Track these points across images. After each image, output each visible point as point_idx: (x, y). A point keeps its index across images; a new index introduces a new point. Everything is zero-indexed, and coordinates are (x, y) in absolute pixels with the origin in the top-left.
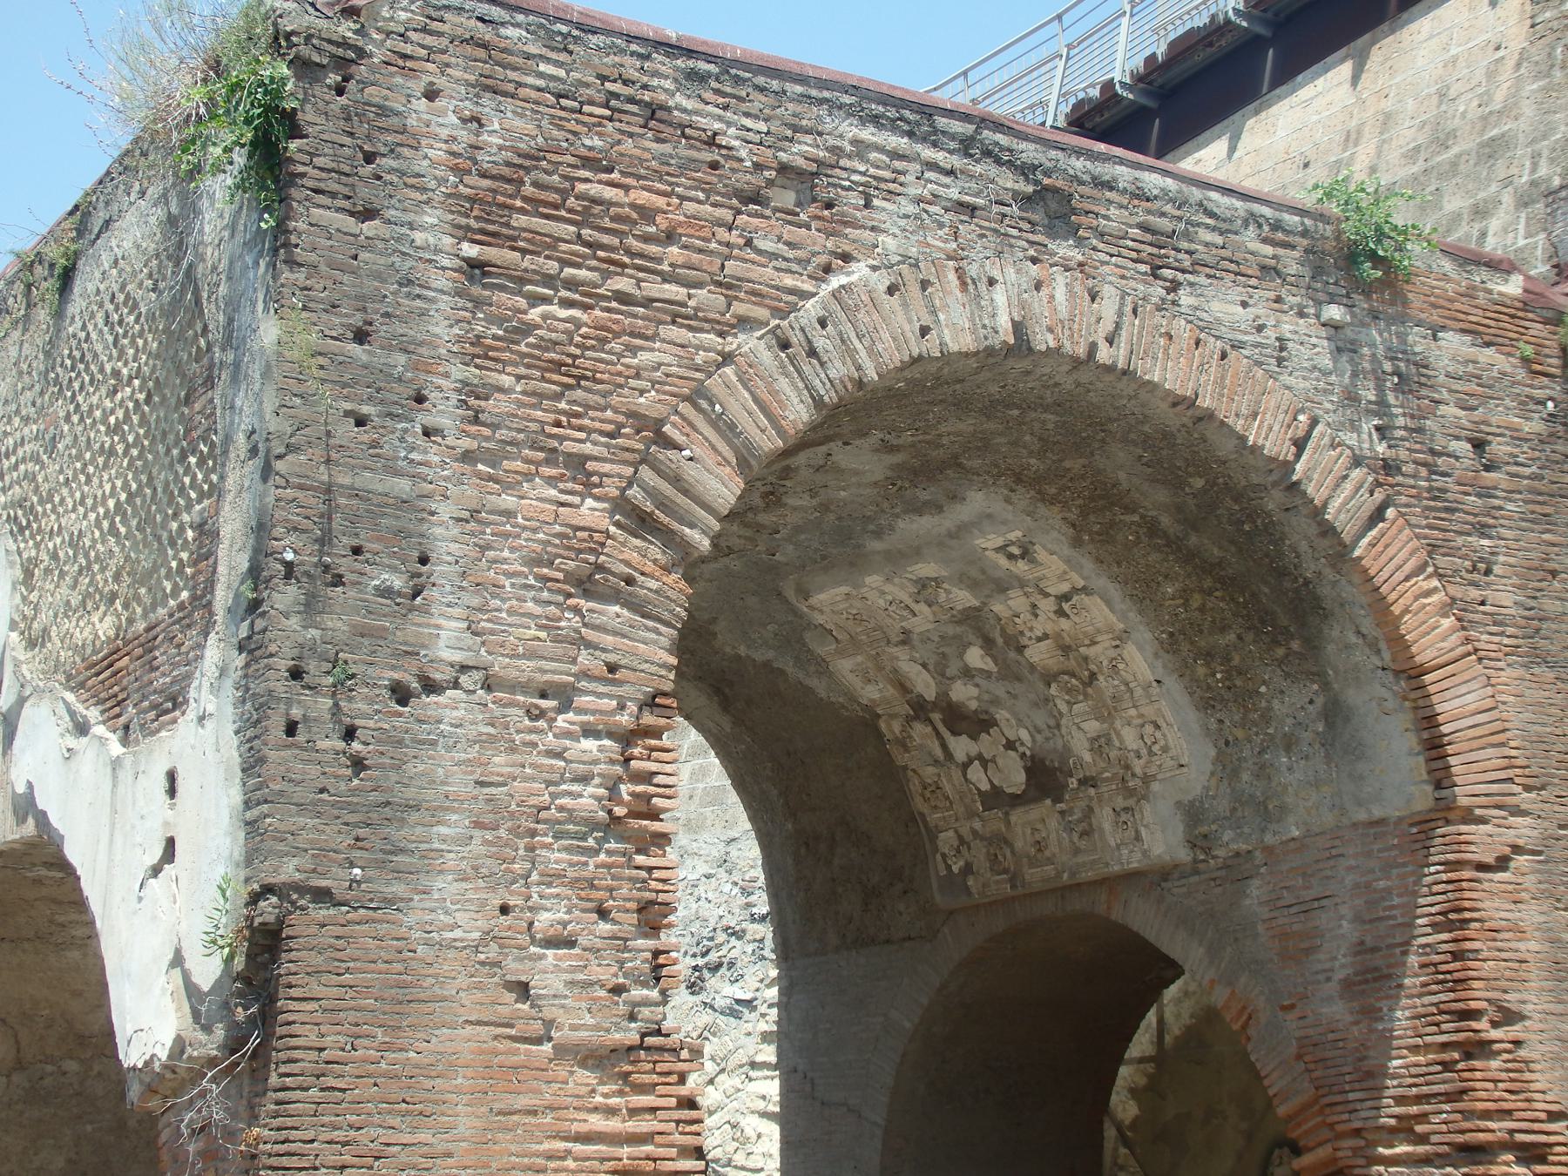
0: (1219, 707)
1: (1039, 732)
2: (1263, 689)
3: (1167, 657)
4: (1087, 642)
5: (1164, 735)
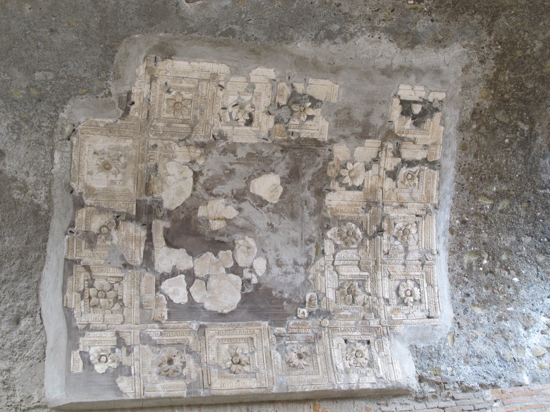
1: (279, 264)
2: (516, 279)
4: (395, 204)
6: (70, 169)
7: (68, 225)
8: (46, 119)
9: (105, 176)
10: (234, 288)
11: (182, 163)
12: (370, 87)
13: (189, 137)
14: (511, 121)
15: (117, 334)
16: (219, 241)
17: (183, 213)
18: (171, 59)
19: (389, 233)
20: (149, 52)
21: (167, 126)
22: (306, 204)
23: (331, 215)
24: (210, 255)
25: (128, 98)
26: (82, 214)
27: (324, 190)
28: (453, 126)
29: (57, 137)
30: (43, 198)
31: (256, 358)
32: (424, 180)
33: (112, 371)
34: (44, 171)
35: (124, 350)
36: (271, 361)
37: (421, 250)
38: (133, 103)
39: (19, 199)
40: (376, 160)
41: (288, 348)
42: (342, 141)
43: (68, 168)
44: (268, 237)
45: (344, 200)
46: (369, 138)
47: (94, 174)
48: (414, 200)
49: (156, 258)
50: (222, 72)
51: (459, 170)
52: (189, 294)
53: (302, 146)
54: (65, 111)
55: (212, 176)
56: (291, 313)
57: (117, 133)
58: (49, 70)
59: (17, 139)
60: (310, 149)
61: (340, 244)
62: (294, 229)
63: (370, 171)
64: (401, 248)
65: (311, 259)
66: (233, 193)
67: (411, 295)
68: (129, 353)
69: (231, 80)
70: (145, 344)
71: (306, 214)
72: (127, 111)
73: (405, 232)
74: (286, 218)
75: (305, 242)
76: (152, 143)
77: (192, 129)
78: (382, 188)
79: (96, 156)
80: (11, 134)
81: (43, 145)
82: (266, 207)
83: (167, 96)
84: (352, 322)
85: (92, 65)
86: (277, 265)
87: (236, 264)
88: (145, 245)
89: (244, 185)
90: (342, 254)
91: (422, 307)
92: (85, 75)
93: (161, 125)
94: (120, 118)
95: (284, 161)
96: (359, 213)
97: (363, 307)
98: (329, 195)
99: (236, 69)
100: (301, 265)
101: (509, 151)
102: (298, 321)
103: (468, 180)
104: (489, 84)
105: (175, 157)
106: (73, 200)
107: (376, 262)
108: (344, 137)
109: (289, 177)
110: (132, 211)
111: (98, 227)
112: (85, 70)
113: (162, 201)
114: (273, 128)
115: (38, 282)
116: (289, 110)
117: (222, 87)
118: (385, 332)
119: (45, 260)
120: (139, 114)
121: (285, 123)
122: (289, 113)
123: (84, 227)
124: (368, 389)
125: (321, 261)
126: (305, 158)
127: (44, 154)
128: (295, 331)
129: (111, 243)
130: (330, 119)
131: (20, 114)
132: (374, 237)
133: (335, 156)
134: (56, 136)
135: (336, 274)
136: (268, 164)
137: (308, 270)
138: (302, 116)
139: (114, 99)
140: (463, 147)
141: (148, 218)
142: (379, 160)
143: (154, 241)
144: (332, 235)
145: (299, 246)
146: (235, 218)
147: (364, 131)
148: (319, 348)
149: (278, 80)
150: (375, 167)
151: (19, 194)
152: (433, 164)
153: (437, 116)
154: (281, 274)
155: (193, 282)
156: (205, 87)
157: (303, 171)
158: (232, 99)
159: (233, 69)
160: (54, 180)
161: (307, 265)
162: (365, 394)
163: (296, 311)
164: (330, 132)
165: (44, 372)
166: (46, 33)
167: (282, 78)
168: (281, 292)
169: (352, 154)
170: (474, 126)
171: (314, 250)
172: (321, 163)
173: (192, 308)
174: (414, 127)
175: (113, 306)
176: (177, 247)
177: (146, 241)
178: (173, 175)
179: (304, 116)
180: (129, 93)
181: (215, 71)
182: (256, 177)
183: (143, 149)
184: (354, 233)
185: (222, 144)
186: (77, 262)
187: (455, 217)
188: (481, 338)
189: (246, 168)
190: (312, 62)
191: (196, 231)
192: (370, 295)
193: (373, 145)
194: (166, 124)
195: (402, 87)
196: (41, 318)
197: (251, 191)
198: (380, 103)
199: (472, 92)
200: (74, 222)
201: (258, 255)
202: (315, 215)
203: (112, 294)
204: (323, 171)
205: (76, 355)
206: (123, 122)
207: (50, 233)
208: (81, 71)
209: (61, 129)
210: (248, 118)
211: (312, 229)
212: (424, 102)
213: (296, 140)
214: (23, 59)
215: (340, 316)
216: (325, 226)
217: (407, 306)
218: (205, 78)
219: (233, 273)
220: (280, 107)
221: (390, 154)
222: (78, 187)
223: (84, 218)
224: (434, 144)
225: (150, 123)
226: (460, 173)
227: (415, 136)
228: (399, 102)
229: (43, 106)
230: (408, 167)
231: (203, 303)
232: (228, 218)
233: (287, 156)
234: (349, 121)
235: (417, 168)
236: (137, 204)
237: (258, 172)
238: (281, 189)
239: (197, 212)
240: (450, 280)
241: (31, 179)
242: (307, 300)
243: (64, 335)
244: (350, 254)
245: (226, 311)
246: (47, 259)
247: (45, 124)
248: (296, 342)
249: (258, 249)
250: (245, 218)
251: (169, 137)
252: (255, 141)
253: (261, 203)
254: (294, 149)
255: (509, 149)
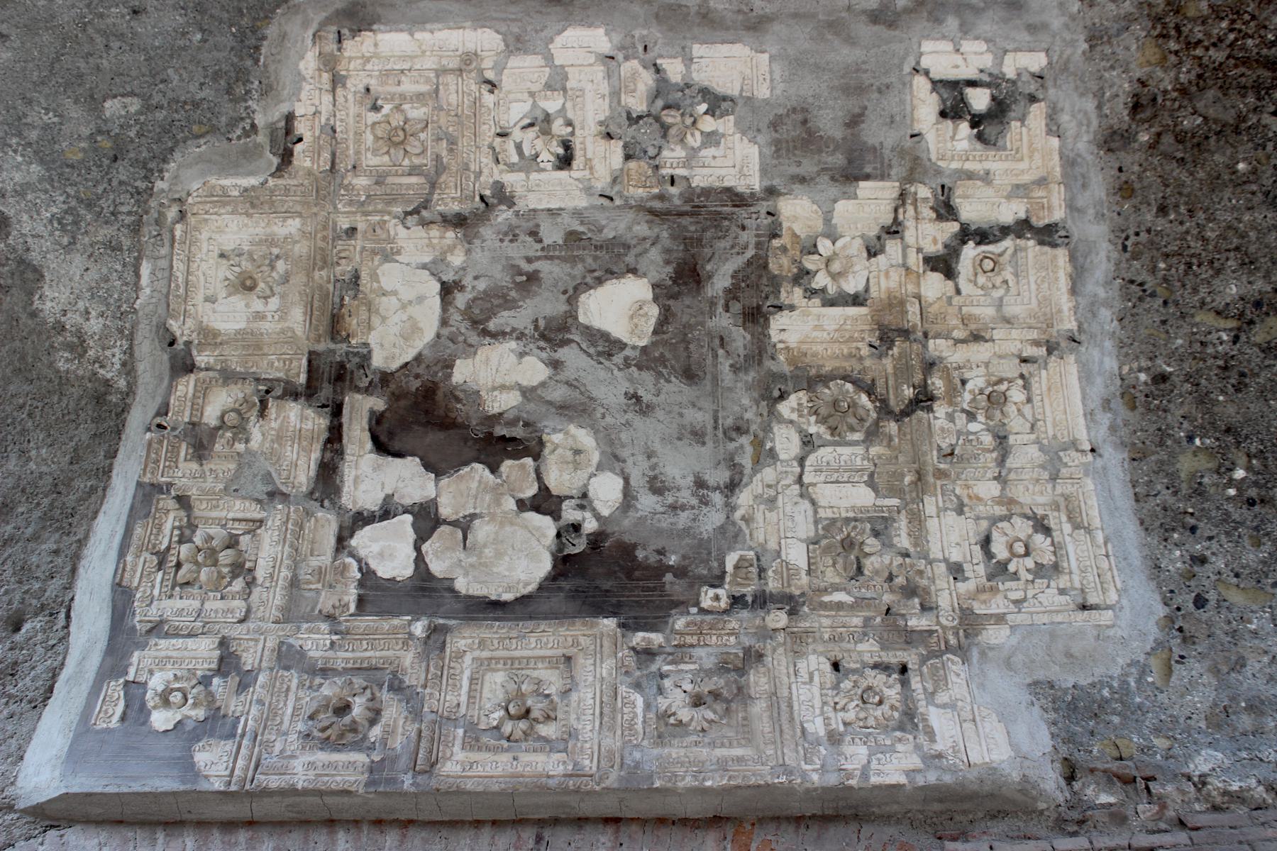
0: (1205, 528)
1: (657, 486)
3: (1133, 417)
4: (957, 334)
5: (1057, 548)
6: (168, 293)
7: (152, 412)
8: (128, 196)
9: (243, 303)
10: (534, 543)
11: (414, 265)
12: (845, 55)
13: (425, 205)
14: (1241, 118)
15: (224, 643)
16: (503, 438)
17: (417, 376)
18: (371, 30)
19: (951, 403)
20: (323, 25)
21: (377, 183)
22: (722, 345)
23: (789, 364)
24: (480, 470)
25: (289, 130)
26: (187, 386)
27: (765, 309)
28: (1085, 138)
29: (148, 231)
30: (118, 366)
31: (574, 704)
32: (1032, 272)
33: (190, 725)
34: (119, 307)
35: (233, 680)
36: (614, 710)
37: (1045, 442)
38: (300, 140)
39: (67, 372)
40: (894, 230)
41: (667, 683)
42: (797, 186)
43: (164, 291)
44: (628, 424)
45: (816, 328)
46: (867, 177)
47: (220, 301)
48: (1008, 321)
49: (346, 478)
50: (487, 47)
51: (1125, 248)
52: (420, 560)
53: (698, 207)
54: (167, 175)
55: (485, 292)
56: (682, 598)
57: (266, 207)
58: (132, 94)
59: (70, 243)
60: (719, 213)
61: (818, 433)
62: (694, 406)
63: (881, 258)
64: (987, 439)
65: (741, 473)
66: (536, 328)
67: (1027, 554)
68: (242, 687)
69: (509, 65)
70: (287, 668)
71: (725, 366)
72: (286, 157)
73: (995, 400)
74: (673, 379)
75: (725, 433)
76: (344, 224)
77: (433, 185)
78: (918, 297)
79: (224, 261)
80: (57, 233)
81: (121, 250)
82: (622, 355)
83: (372, 117)
84: (857, 621)
85: (216, 73)
86: (650, 489)
87: (544, 490)
88: (324, 450)
89: (563, 307)
90: (824, 454)
91: (1063, 581)
92: (201, 95)
93: (361, 182)
94: (272, 175)
95: (659, 246)
96: (861, 359)
97: (886, 585)
98: (777, 317)
99: (518, 39)
100: (715, 489)
101: (1253, 193)
102: (699, 618)
103: (1153, 270)
104: (1159, 27)
105: (399, 253)
106: (171, 358)
107: (920, 476)
108: (802, 180)
109: (675, 282)
110: (298, 376)
111: (219, 414)
112: (202, 84)
113: (370, 352)
114: (622, 170)
115: (82, 543)
116: (656, 126)
117: (492, 86)
118: (953, 641)
119: (104, 496)
120: (313, 161)
121: (651, 158)
122: (658, 135)
123: (187, 414)
124: (897, 787)
125: (768, 474)
126: (709, 234)
127: (119, 267)
128: (689, 640)
129: (247, 448)
130: (760, 138)
131: (78, 191)
132: (906, 413)
133: (785, 225)
134: (145, 230)
135: (806, 505)
136: (619, 255)
137: (733, 500)
138: (689, 136)
139: (261, 138)
140: (1125, 190)
141: (335, 391)
142: (900, 229)
143: (345, 441)
144: (793, 410)
145: (710, 444)
146: (543, 384)
147: (850, 161)
148: (757, 681)
149: (620, 57)
150: (893, 246)
151: (67, 360)
152: (1048, 235)
153: (1037, 114)
154: (662, 510)
155: (434, 529)
156: (453, 88)
157: (708, 267)
158: (517, 111)
159: (511, 40)
160: (138, 323)
161: (732, 487)
162: (895, 807)
163: (698, 595)
164: (764, 171)
165: (34, 730)
166: (123, 16)
167: (627, 50)
168: (661, 552)
169: (828, 220)
170: (1144, 137)
171: (749, 450)
172: (751, 246)
173: (423, 589)
174: (979, 146)
175: (230, 584)
176: (399, 455)
177: (329, 440)
178: (395, 293)
179: (693, 135)
180: (290, 118)
181: (470, 47)
182: (591, 288)
183: (324, 238)
184: (853, 405)
185: (503, 215)
186: (158, 488)
187: (1135, 365)
188: (1258, 666)
189: (567, 267)
190: (698, 13)
191: (447, 416)
192: (907, 555)
193: (879, 194)
194: (374, 180)
195: (927, 46)
196: (68, 617)
197: (582, 319)
198: (880, 91)
199: (1119, 50)
200: (168, 405)
201: (600, 467)
202: (746, 371)
203: (226, 557)
204: (759, 264)
205: (115, 689)
206: (280, 182)
207: (123, 437)
208: (193, 87)
209: (156, 215)
210: (561, 151)
211: (743, 403)
212: (992, 81)
213: (681, 194)
214: (80, 76)
215: (824, 606)
216: (776, 394)
217: (1018, 579)
218: (451, 66)
219: (537, 509)
220: (634, 120)
221: (927, 213)
222: (182, 329)
223: (190, 395)
224: (1042, 182)
225: (338, 180)
226: (1128, 255)
227: (988, 165)
228: (929, 86)
229: (122, 172)
230: (978, 244)
231: (452, 580)
232: (525, 383)
233: (665, 234)
234: (809, 140)
235: (1008, 243)
236: (310, 362)
237: (596, 274)
238: (654, 311)
239: (450, 376)
240: (1142, 523)
241: (94, 325)
242: (729, 567)
243: (102, 644)
244: (851, 454)
245: (508, 597)
246: (109, 492)
247: (124, 209)
248: (692, 667)
249: (602, 453)
250: (568, 383)
251: (380, 207)
252: (581, 202)
253: (605, 345)
254: (681, 214)
255: (1254, 187)
